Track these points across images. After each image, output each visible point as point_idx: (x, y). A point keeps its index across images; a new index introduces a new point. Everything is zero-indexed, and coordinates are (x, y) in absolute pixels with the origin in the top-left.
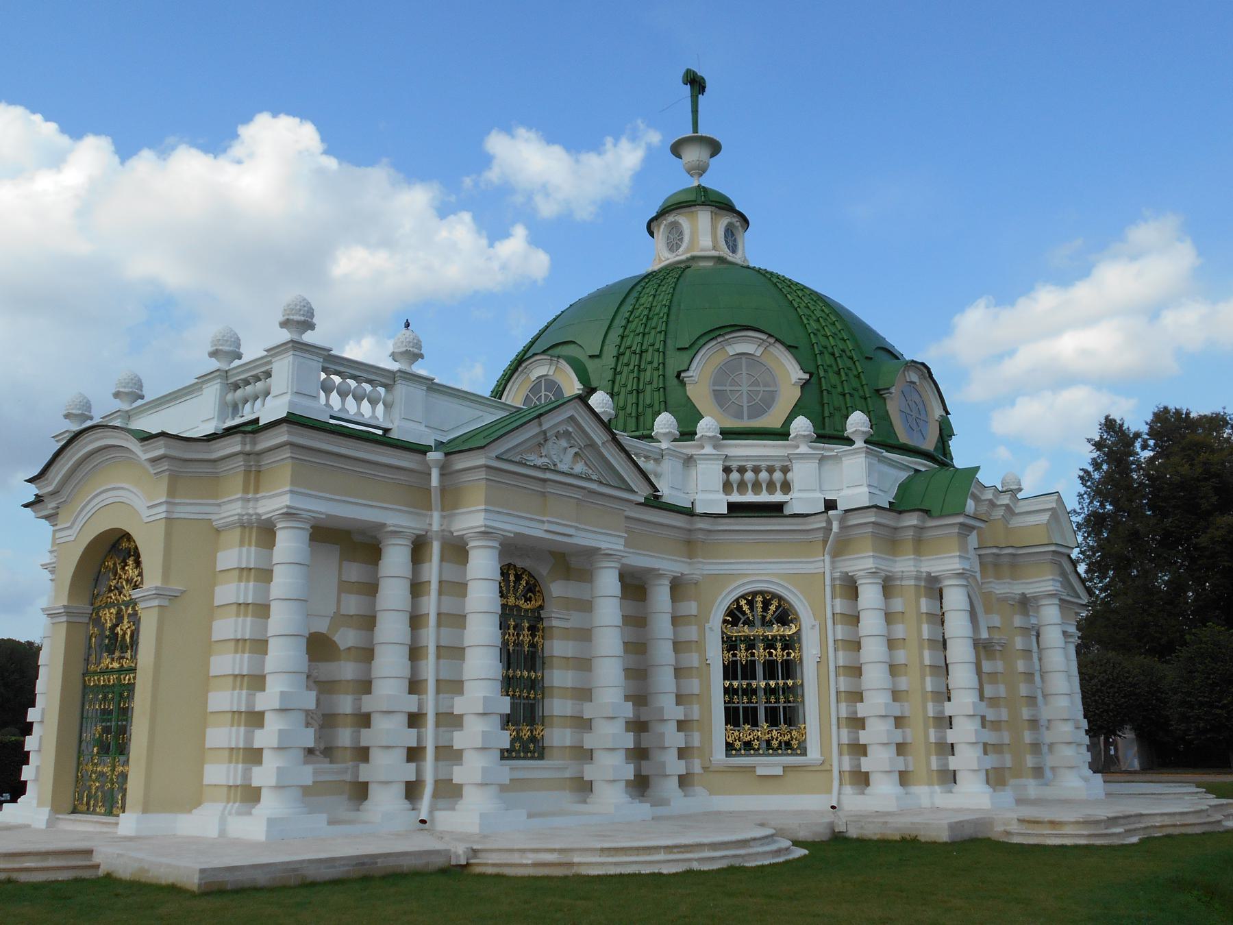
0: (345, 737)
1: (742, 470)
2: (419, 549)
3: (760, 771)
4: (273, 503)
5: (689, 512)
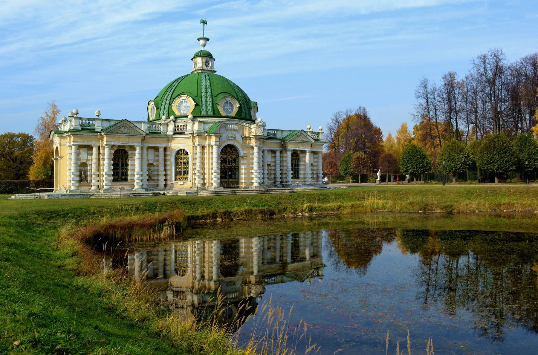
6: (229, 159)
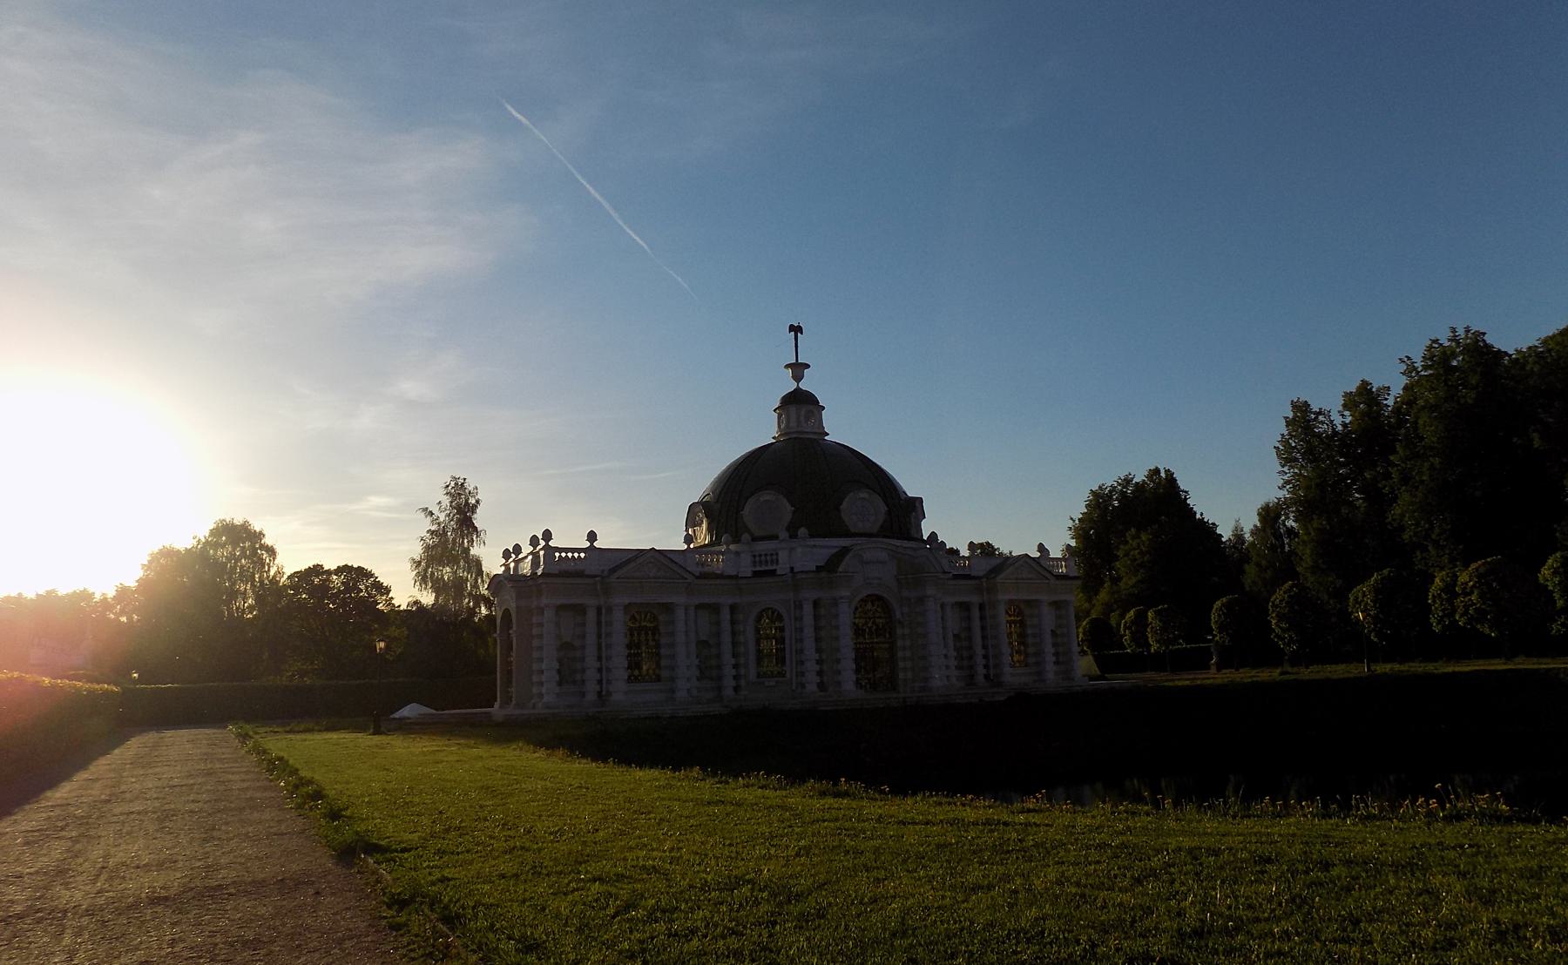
0: (578, 677)
1: (760, 555)
2: (599, 610)
3: (767, 684)
4: (544, 601)
5: (736, 577)
6: (870, 628)
